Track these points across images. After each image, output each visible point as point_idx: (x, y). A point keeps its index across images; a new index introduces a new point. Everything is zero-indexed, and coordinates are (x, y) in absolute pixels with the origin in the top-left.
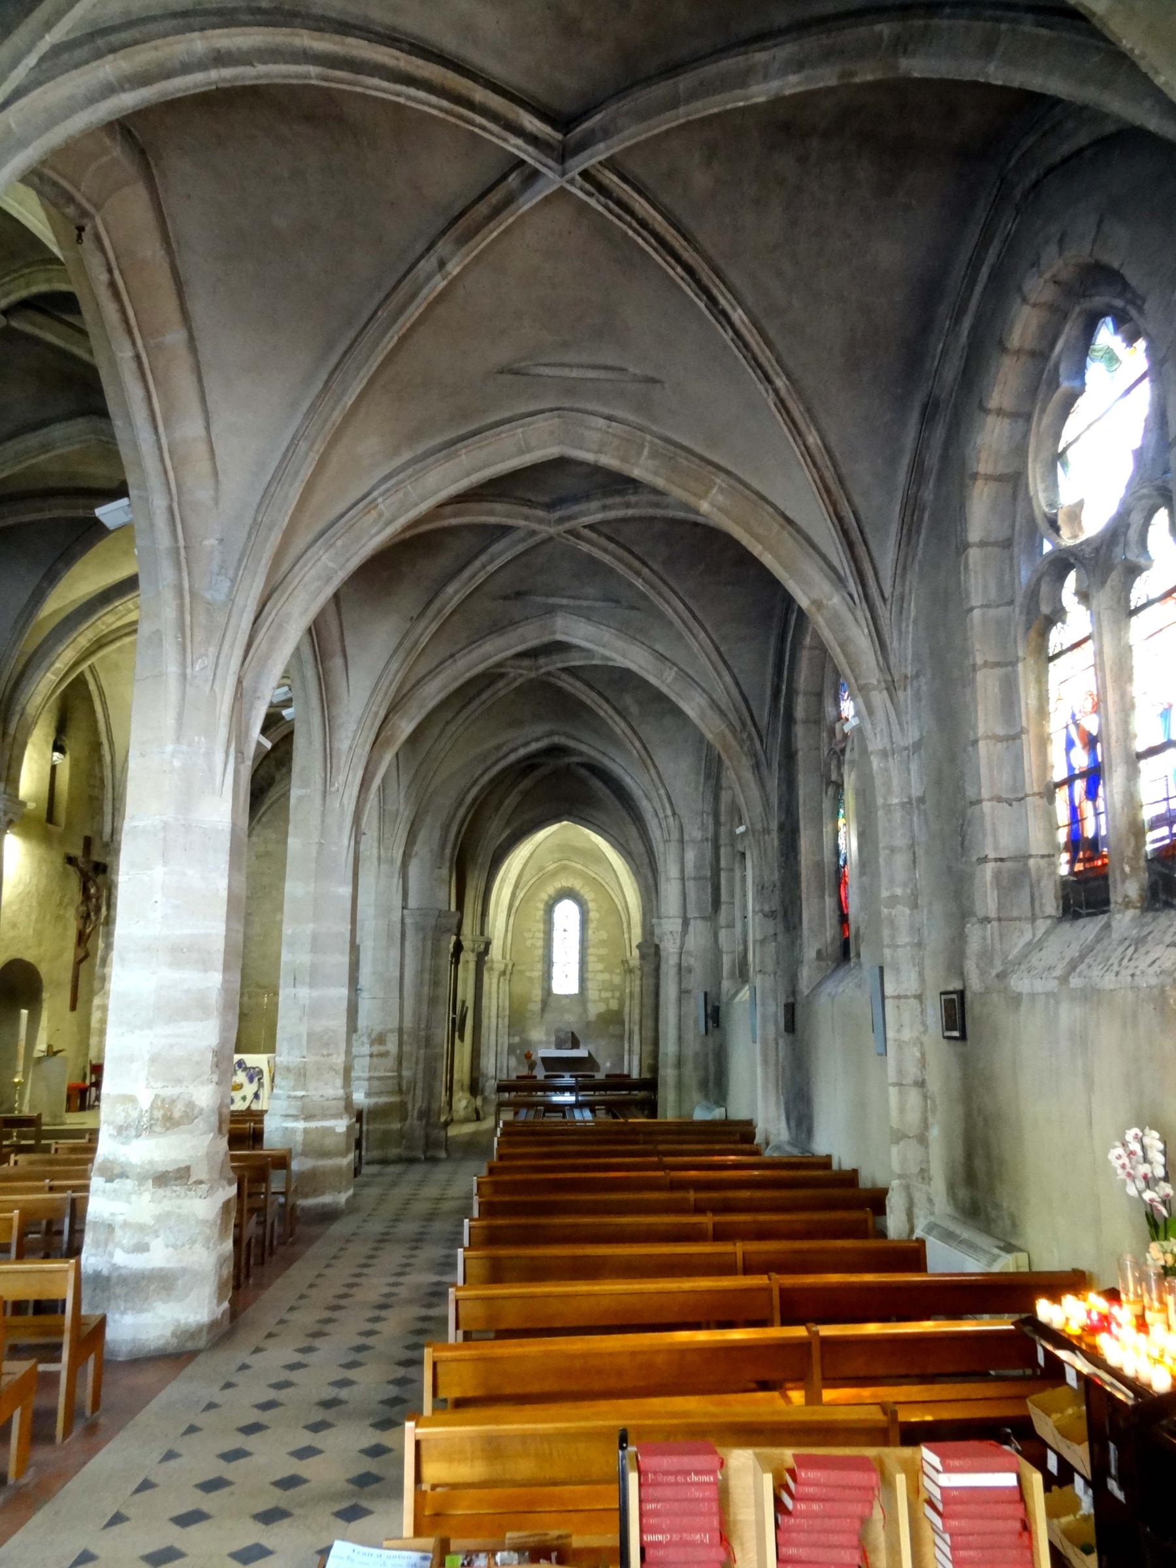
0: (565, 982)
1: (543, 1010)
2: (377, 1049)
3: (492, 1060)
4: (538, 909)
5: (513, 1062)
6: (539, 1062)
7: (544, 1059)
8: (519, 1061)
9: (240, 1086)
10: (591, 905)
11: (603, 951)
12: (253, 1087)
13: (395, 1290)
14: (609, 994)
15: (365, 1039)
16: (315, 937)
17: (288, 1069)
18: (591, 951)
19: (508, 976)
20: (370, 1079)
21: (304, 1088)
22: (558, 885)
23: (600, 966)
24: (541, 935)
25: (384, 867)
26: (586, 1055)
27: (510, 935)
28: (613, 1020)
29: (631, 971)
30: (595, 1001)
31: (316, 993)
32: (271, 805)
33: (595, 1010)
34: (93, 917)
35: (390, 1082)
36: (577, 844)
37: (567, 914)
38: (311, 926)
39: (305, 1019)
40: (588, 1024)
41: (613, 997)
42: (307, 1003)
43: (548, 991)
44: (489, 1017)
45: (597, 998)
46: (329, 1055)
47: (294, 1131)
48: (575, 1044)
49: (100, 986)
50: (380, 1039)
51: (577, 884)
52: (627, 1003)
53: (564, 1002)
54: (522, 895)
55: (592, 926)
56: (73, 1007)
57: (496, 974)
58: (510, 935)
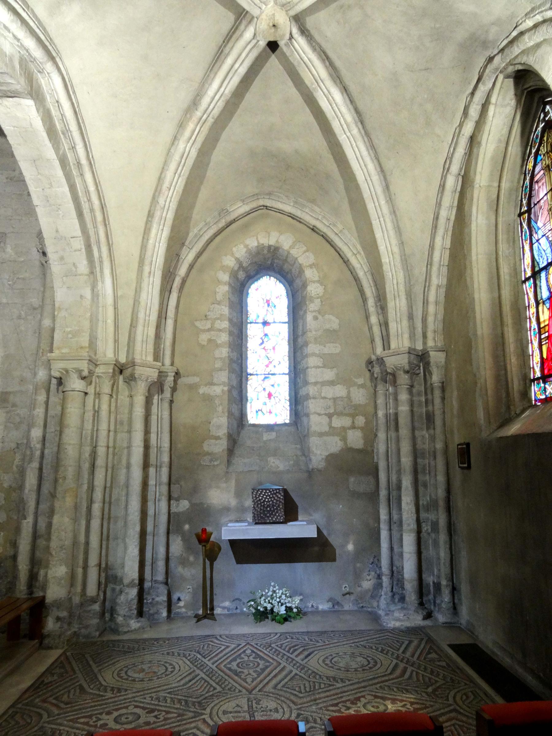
0: (268, 404)
1: (231, 452)
3: (133, 551)
4: (219, 282)
5: (177, 546)
6: (226, 549)
7: (233, 543)
8: (188, 548)
10: (309, 274)
11: (333, 349)
14: (346, 422)
18: (312, 348)
19: (167, 394)
22: (252, 243)
23: (329, 375)
24: (225, 324)
26: (312, 533)
27: (170, 323)
28: (357, 466)
29: (389, 377)
30: (321, 435)
33: (321, 449)
36: (286, 146)
37: (267, 296)
40: (310, 473)
41: (353, 427)
43: (240, 419)
44: (128, 466)
45: (326, 429)
48: (290, 513)
51: (285, 241)
52: (382, 435)
53: (266, 437)
54: (191, 257)
55: (313, 306)
57: (141, 389)
58: (170, 323)
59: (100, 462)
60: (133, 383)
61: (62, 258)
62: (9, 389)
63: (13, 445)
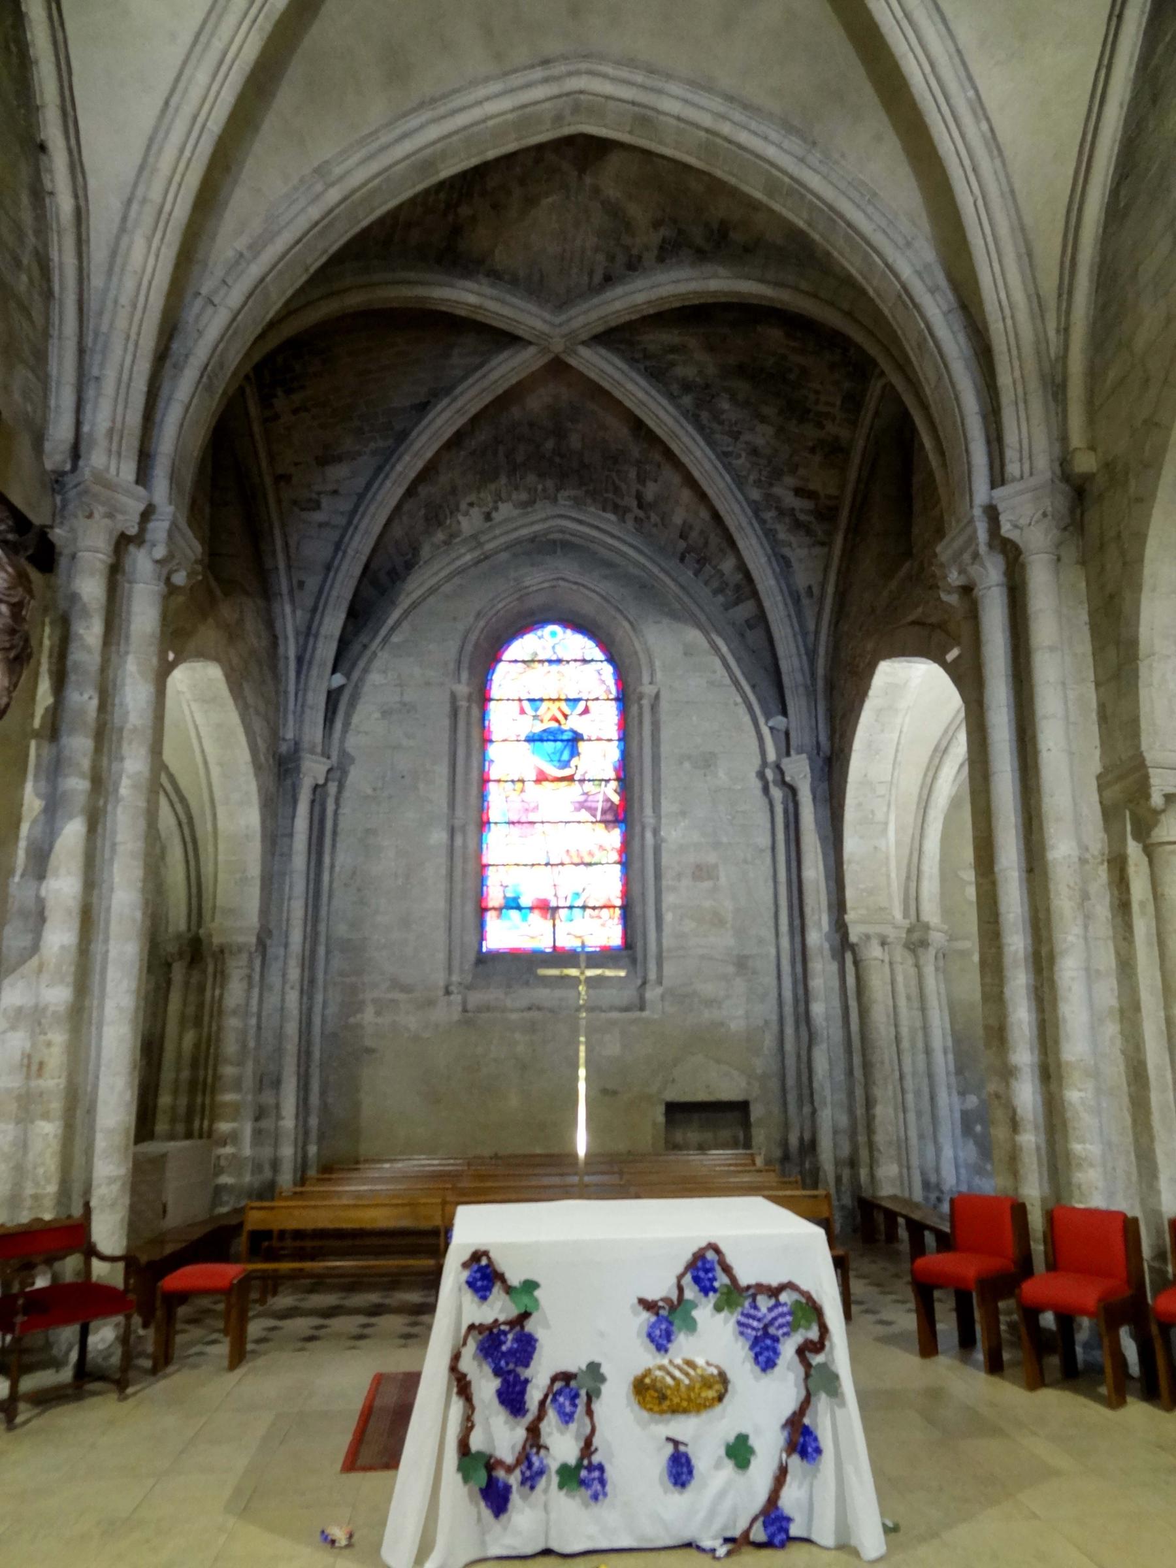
32: (414, 605)
49: (25, 941)
59: (905, 1044)
60: (920, 951)
61: (860, 804)
62: (745, 952)
63: (761, 1023)
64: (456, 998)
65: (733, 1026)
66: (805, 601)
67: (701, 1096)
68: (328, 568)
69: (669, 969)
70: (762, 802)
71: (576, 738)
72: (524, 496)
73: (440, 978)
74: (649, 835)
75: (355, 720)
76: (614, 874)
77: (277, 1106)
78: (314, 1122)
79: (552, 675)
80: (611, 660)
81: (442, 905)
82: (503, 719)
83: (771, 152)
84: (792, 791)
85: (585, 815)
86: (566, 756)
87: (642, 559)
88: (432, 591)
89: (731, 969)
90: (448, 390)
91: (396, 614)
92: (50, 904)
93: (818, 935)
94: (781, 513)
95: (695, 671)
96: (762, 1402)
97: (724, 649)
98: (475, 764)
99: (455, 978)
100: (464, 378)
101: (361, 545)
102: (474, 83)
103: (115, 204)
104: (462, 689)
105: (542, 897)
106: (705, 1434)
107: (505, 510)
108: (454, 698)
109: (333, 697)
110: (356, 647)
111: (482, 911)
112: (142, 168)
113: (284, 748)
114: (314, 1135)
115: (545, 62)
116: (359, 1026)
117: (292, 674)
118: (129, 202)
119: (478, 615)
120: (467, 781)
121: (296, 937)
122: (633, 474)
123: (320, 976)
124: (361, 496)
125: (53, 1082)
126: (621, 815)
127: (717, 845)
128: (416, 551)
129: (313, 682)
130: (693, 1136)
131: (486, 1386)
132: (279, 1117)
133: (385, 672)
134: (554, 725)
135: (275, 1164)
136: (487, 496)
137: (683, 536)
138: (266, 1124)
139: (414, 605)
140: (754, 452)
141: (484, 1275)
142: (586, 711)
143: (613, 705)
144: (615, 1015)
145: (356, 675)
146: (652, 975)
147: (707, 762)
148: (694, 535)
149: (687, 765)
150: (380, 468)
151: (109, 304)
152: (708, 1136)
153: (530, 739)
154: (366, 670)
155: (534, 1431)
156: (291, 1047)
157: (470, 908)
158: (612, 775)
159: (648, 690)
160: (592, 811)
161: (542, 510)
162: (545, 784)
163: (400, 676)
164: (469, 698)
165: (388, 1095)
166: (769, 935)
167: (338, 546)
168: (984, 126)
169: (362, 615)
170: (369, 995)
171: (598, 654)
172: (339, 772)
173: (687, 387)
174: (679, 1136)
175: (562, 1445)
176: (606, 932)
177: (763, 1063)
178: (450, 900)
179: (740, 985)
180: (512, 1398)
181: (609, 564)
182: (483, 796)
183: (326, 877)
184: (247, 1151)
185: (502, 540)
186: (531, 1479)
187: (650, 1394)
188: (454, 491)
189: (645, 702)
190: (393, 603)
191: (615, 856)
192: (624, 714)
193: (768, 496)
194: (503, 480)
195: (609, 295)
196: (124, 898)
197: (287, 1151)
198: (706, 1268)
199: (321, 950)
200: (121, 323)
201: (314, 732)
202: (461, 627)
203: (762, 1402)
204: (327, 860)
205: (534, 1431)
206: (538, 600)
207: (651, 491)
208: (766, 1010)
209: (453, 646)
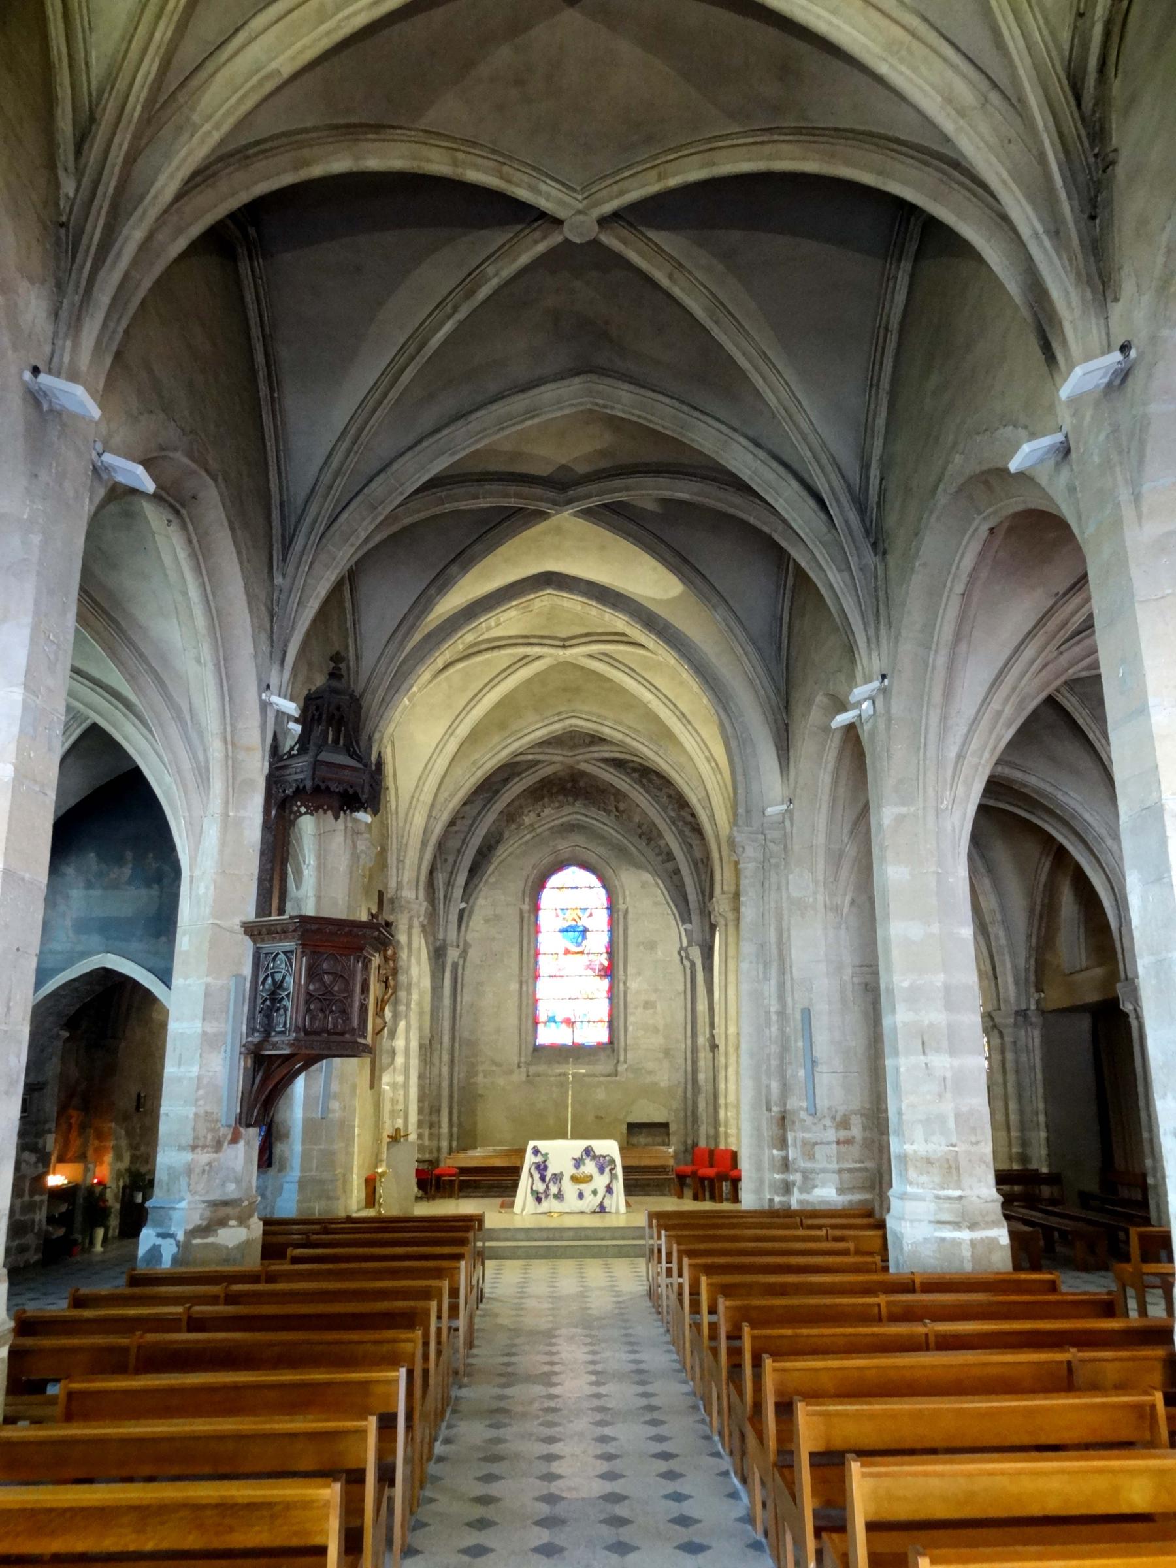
2: (843, 1134)
9: (588, 1179)
12: (605, 1179)
13: (499, 1391)
15: (828, 1122)
16: (947, 988)
17: (929, 1161)
20: (840, 1171)
21: (959, 1186)
25: (831, 915)
31: (956, 1062)
34: (391, 983)
35: (860, 1174)
38: (941, 977)
39: (949, 1095)
42: (949, 1075)
46: (977, 1143)
47: (956, 1243)
50: (844, 1124)
56: (372, 1086)
64: (523, 1069)
65: (662, 1084)
66: (700, 865)
67: (645, 1120)
68: (459, 851)
69: (630, 1055)
70: (680, 967)
71: (585, 931)
72: (557, 804)
73: (516, 1060)
74: (621, 985)
75: (471, 924)
76: (605, 1005)
77: (439, 1122)
78: (455, 1130)
79: (573, 896)
80: (604, 886)
81: (516, 1022)
82: (548, 920)
83: (645, 750)
84: (693, 964)
85: (590, 972)
86: (580, 940)
87: (619, 837)
88: (511, 854)
89: (661, 1055)
90: (519, 774)
91: (492, 868)
92: (397, 1049)
93: (702, 1040)
94: (686, 823)
95: (646, 895)
96: (600, 1182)
97: (662, 885)
98: (532, 945)
99: (523, 1059)
100: (526, 770)
101: (476, 842)
102: (531, 724)
103: (408, 797)
104: (526, 907)
105: (567, 1015)
106: (587, 1188)
107: (547, 811)
108: (521, 912)
109: (461, 913)
110: (471, 886)
111: (536, 1023)
112: (417, 787)
113: (438, 944)
114: (455, 1136)
115: (559, 714)
116: (475, 1084)
117: (442, 906)
118: (413, 797)
119: (534, 867)
120: (528, 955)
121: (446, 1039)
122: (612, 798)
123: (456, 1059)
124: (475, 819)
125: (401, 1107)
126: (608, 971)
127: (656, 991)
128: (501, 835)
129: (451, 909)
130: (642, 1140)
131: (537, 1176)
132: (440, 1127)
133: (486, 898)
134: (574, 923)
135: (439, 1149)
136: (538, 806)
137: (639, 826)
138: (435, 1131)
139: (501, 862)
140: (670, 796)
141: (536, 1152)
142: (591, 915)
143: (605, 912)
144: (602, 1079)
145: (471, 902)
146: (622, 1059)
147: (651, 946)
148: (645, 827)
149: (641, 948)
150: (485, 806)
151: (406, 834)
152: (650, 1140)
153: (562, 931)
154: (477, 898)
155: (547, 1187)
156: (445, 1093)
157: (530, 1022)
158: (604, 950)
159: (622, 907)
160: (593, 970)
161: (567, 810)
162: (569, 956)
163: (494, 900)
164: (529, 912)
165: (495, 1118)
166: (681, 1037)
167: (464, 841)
168: (713, 764)
169: (475, 870)
170: (480, 1068)
171: (598, 884)
172: (464, 954)
173: (634, 770)
174: (635, 1140)
175: (554, 1189)
176: (600, 1035)
177: (676, 1104)
178: (520, 1019)
179: (666, 1064)
180: (543, 1178)
181: (603, 838)
182: (536, 962)
183: (458, 1008)
184: (427, 1143)
185: (547, 826)
186: (547, 1196)
187: (574, 1179)
188: (521, 807)
189: (621, 914)
190: (490, 862)
191: (605, 995)
192: (611, 916)
193: (679, 816)
194: (546, 800)
195: (592, 749)
196: (414, 1045)
197: (444, 1144)
198: (588, 1151)
199: (457, 1045)
200: (411, 842)
201: (452, 935)
202: (525, 873)
203: (600, 1182)
204: (459, 999)
205: (547, 1187)
206: (566, 855)
207: (622, 806)
208: (680, 1076)
209: (521, 884)
